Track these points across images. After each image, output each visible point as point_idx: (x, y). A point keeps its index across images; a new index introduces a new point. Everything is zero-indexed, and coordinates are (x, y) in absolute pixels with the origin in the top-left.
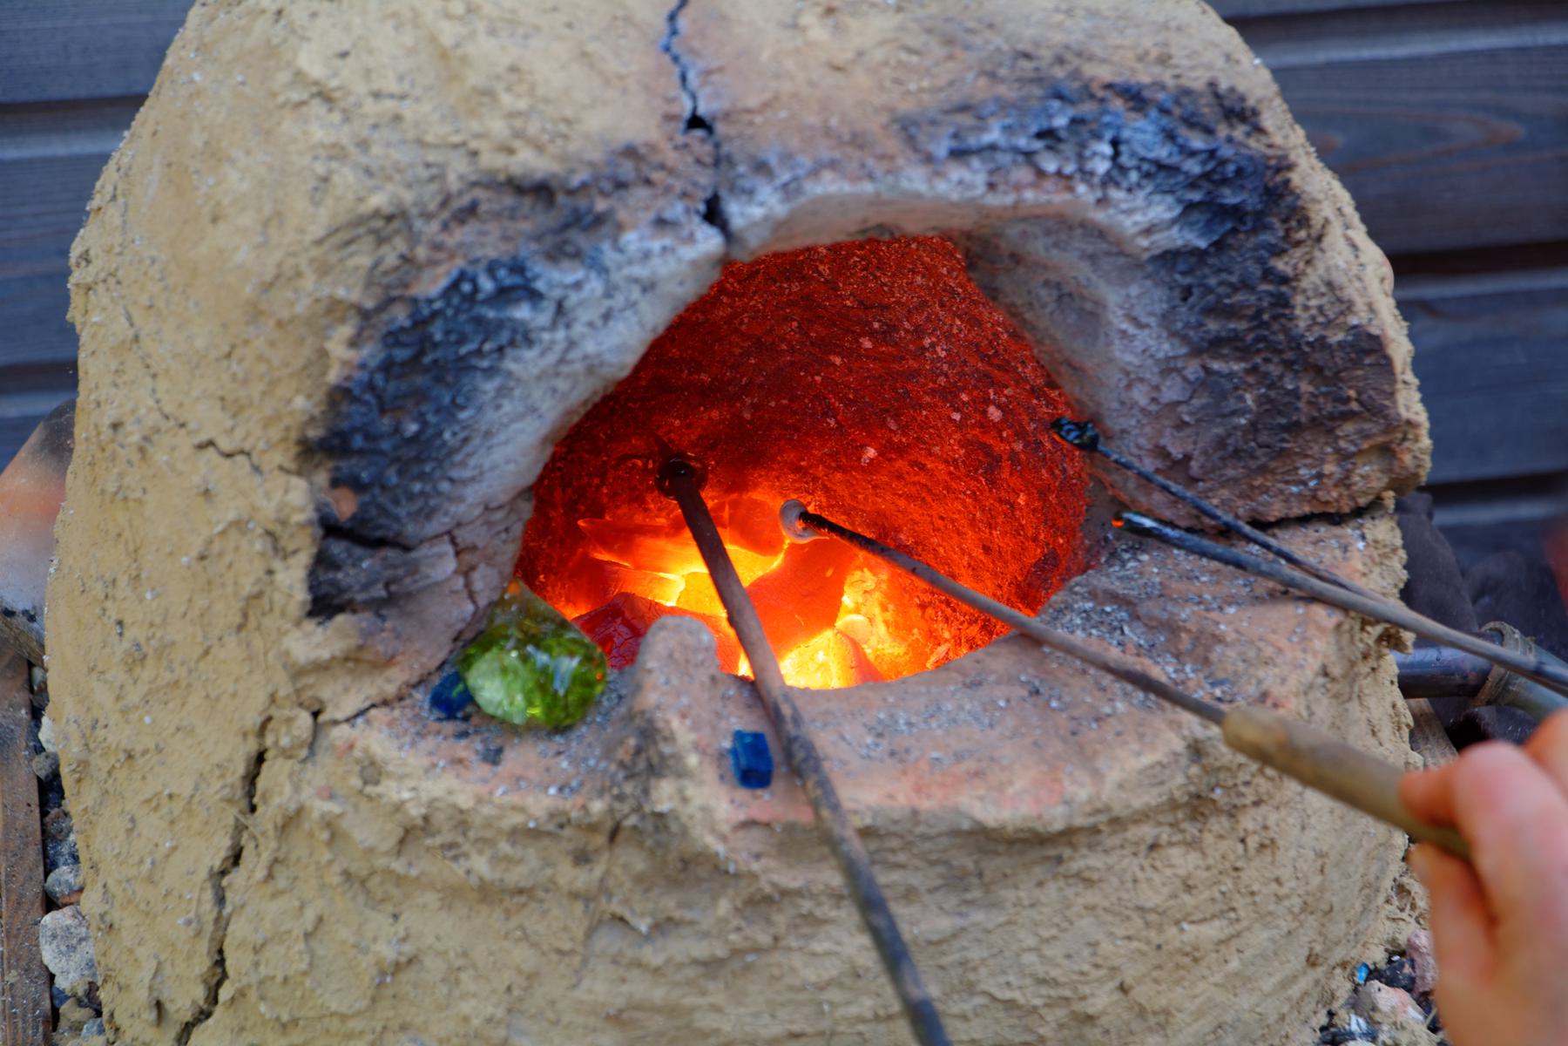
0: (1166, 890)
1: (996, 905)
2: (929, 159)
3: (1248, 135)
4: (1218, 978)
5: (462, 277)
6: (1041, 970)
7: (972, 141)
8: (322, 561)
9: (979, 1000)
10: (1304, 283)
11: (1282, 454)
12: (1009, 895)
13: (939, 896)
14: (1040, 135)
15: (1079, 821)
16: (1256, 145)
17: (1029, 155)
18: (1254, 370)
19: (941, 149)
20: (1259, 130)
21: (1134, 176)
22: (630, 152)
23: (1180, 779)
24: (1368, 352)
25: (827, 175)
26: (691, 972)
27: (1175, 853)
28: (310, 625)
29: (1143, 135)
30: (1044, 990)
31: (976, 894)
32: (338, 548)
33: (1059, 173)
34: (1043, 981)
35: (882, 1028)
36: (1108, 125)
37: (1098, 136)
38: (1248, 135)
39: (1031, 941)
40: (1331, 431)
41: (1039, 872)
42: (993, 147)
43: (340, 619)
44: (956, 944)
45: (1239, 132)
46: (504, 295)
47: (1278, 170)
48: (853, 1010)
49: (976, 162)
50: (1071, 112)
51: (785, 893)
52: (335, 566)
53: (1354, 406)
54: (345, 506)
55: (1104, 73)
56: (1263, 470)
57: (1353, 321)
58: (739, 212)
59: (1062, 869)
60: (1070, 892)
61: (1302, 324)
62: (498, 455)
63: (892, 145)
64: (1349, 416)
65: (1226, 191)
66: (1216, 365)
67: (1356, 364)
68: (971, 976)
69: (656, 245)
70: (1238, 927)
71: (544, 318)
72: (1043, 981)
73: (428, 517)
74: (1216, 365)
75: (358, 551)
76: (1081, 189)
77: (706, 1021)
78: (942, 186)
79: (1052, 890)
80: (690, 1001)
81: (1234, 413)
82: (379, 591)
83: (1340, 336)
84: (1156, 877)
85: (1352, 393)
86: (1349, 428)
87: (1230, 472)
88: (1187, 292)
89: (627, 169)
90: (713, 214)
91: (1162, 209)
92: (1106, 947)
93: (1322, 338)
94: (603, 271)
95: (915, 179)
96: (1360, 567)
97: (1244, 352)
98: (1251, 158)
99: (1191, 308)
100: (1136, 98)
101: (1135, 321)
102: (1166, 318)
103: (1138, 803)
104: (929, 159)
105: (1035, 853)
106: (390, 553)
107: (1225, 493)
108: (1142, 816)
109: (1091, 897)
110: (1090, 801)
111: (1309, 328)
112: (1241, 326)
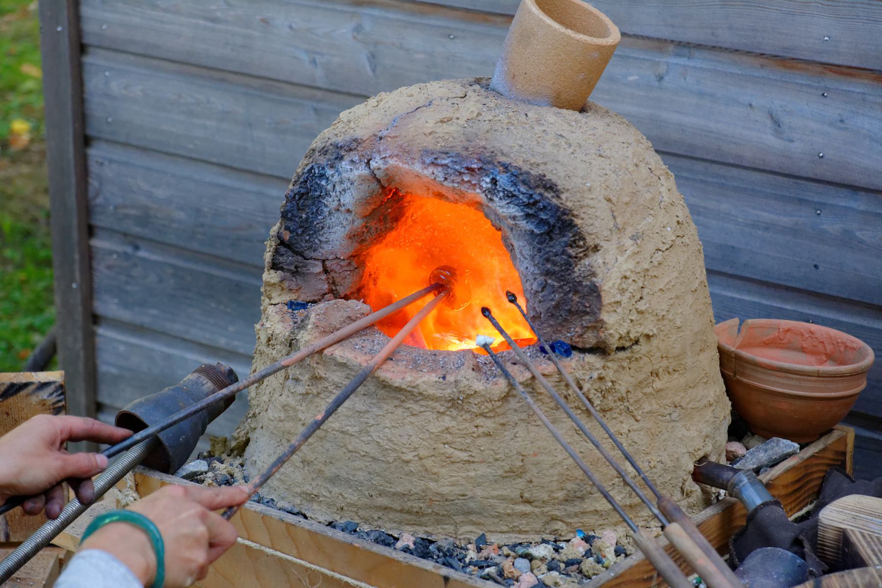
0: (440, 429)
1: (380, 408)
2: (424, 163)
3: (553, 197)
4: (464, 475)
5: (312, 168)
6: (390, 436)
7: (439, 161)
8: (276, 252)
9: (370, 438)
10: (582, 261)
11: (566, 320)
12: (385, 407)
13: (365, 398)
14: (467, 169)
15: (404, 386)
16: (555, 201)
17: (461, 173)
18: (561, 287)
19: (428, 161)
20: (558, 197)
21: (501, 194)
22: (355, 140)
23: (449, 391)
24: (595, 292)
25: (395, 159)
26: (299, 397)
27: (447, 418)
28: (272, 271)
29: (503, 179)
30: (390, 444)
31: (375, 401)
32: (283, 249)
33: (469, 182)
34: (390, 440)
35: (341, 435)
36: (492, 173)
37: (487, 175)
38: (553, 197)
39: (389, 425)
40: (581, 317)
41: (397, 402)
42: (446, 165)
43: (279, 272)
44: (366, 416)
45: (549, 195)
46: (322, 176)
47: (564, 214)
48: (333, 425)
49: (440, 169)
50: (480, 165)
51: (321, 378)
52: (282, 255)
53: (588, 310)
54: (287, 236)
55: (503, 159)
56: (560, 325)
57: (594, 279)
58: (373, 164)
59: (404, 404)
60: (406, 414)
61: (576, 275)
62: (332, 237)
63: (417, 156)
64: (588, 313)
65: (542, 213)
66: (549, 281)
67: (590, 294)
68: (369, 429)
69: (349, 167)
70: (472, 459)
71: (329, 187)
72: (390, 440)
73: (314, 251)
74: (549, 281)
75: (290, 253)
76: (478, 190)
77: (301, 416)
78: (426, 172)
79: (400, 410)
80: (298, 407)
81: (552, 300)
82: (293, 268)
83: (588, 283)
84: (437, 423)
85: (587, 305)
86: (587, 317)
87: (552, 323)
88: (540, 250)
89: (354, 145)
90: (368, 163)
91: (514, 210)
92: (413, 438)
93: (580, 282)
94: (340, 174)
95: (417, 167)
96: (573, 365)
97: (559, 280)
98: (549, 204)
99: (541, 257)
100: (506, 168)
101: (522, 255)
102: (533, 257)
103: (431, 392)
104: (424, 163)
105: (393, 394)
106: (300, 258)
107: (549, 329)
108: (436, 399)
109: (412, 419)
110: (410, 382)
111: (578, 277)
112: (557, 269)
